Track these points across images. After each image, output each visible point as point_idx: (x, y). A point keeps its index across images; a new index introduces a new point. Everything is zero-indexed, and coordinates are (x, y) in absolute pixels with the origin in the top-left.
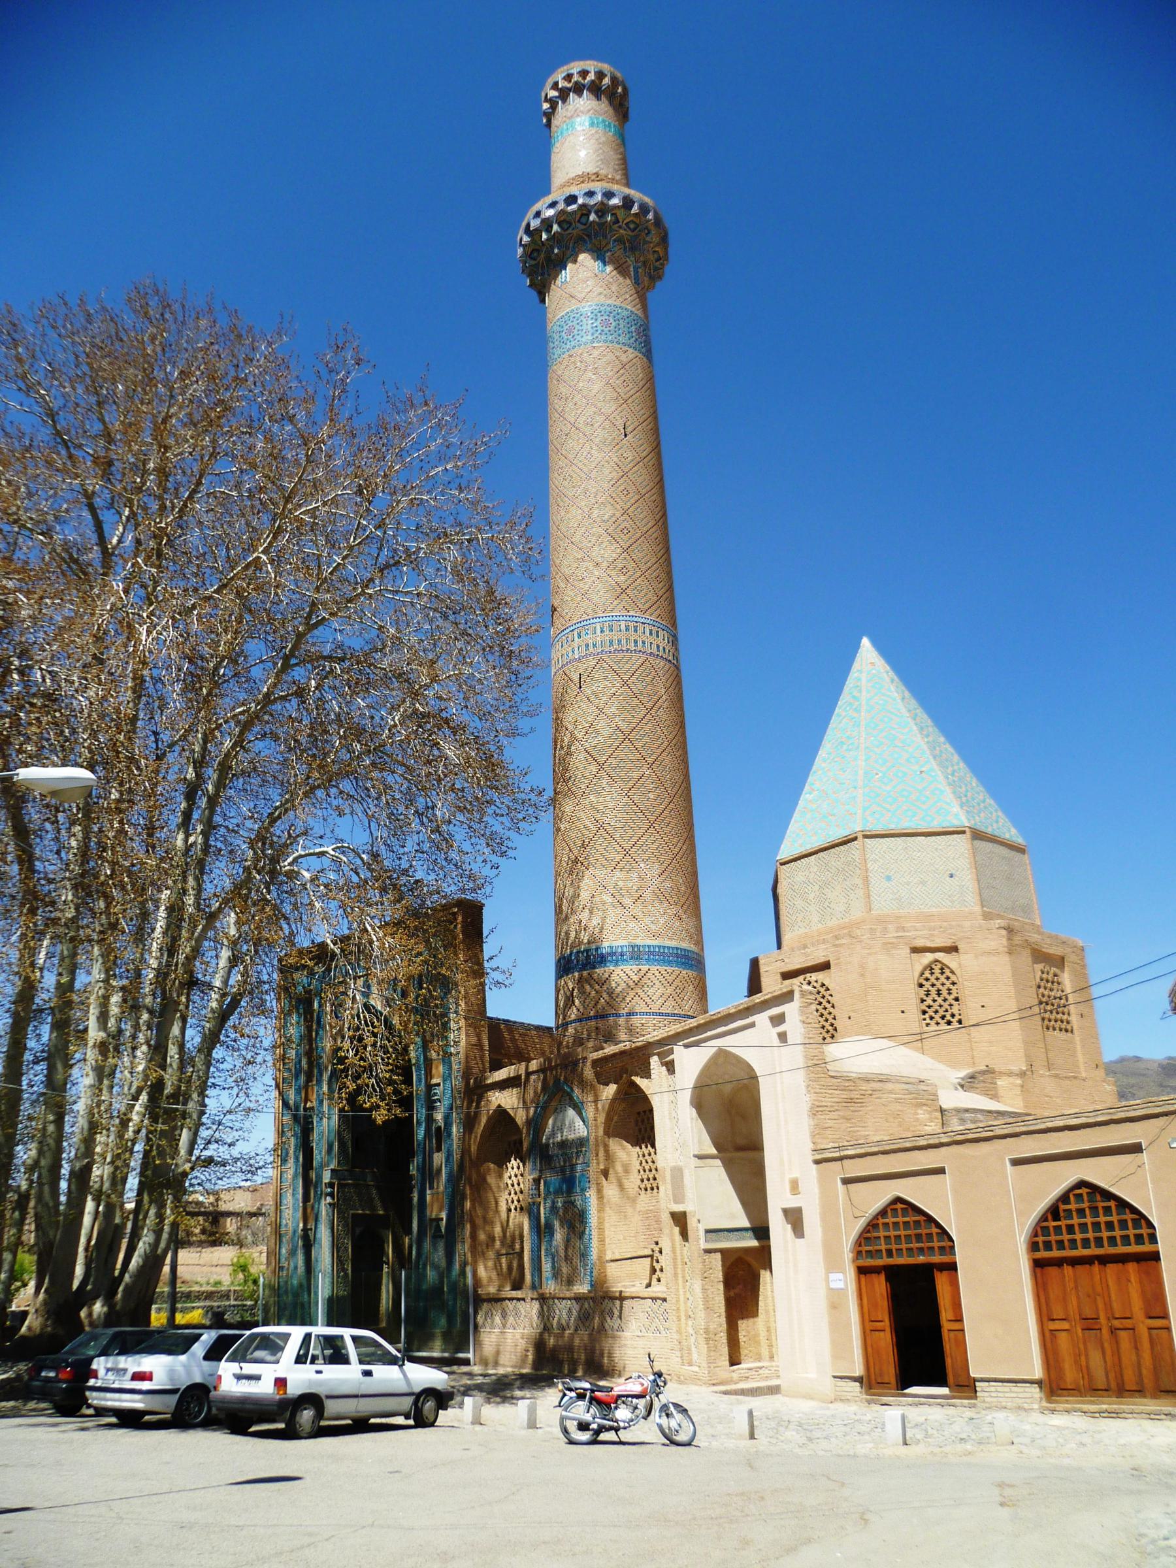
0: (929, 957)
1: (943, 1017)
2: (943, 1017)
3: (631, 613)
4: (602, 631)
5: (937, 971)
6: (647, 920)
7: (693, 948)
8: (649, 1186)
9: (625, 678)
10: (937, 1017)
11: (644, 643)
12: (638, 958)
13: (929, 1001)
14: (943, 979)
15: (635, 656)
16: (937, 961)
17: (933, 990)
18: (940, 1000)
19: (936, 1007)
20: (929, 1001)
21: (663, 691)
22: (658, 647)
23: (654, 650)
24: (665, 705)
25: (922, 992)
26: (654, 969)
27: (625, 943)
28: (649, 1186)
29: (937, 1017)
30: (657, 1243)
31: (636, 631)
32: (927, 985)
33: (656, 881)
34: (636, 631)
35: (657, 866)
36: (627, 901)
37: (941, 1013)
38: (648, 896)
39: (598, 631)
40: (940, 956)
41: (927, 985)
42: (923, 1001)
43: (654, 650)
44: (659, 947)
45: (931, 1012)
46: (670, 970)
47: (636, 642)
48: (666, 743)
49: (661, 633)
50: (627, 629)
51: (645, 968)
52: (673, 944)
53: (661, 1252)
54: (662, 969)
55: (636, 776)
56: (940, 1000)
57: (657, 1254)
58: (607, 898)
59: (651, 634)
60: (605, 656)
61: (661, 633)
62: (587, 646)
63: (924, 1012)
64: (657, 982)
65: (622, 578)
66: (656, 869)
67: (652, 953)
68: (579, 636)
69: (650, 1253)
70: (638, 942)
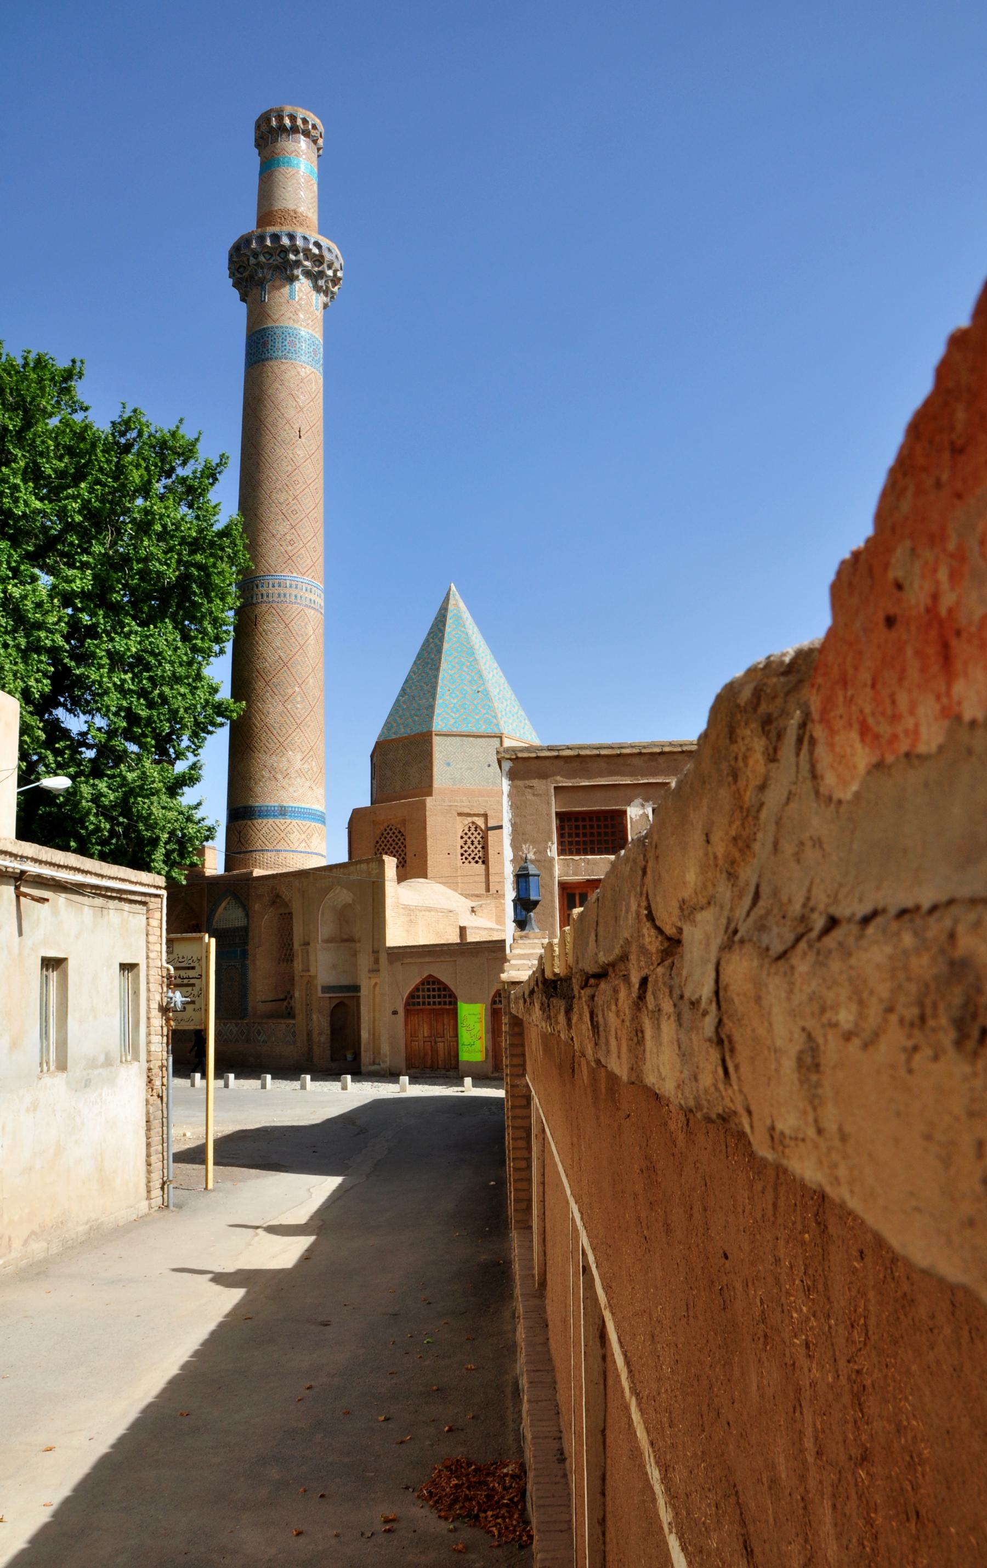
0: (470, 819)
1: (473, 858)
2: (473, 858)
5: (473, 829)
6: (291, 789)
10: (470, 858)
12: (285, 815)
13: (466, 848)
14: (476, 834)
16: (473, 823)
17: (469, 841)
18: (472, 847)
19: (470, 851)
20: (466, 848)
25: (461, 842)
26: (294, 822)
27: (276, 804)
29: (470, 858)
32: (466, 838)
35: (300, 754)
36: (279, 776)
37: (473, 855)
41: (466, 838)
42: (462, 847)
45: (466, 855)
46: (304, 823)
49: (314, 589)
50: (291, 586)
51: (288, 821)
54: (299, 822)
56: (472, 847)
60: (274, 605)
63: (462, 855)
65: (290, 548)
66: (299, 756)
70: (285, 804)
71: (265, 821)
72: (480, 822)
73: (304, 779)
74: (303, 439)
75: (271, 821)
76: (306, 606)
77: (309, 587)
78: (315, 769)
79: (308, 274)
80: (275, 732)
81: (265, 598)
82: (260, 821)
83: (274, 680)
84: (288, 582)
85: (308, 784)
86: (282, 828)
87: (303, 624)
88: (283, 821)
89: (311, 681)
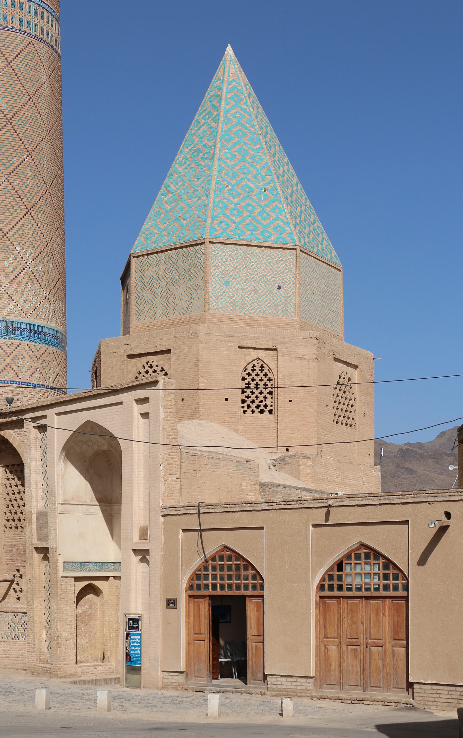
6: (20, 299)
7: (60, 329)
8: (14, 526)
9: (10, 59)
11: (29, 23)
12: (11, 333)
15: (20, 37)
21: (45, 77)
22: (42, 30)
23: (38, 33)
24: (47, 92)
26: (25, 343)
28: (14, 526)
30: (18, 571)
38: (22, 278)
43: (38, 33)
46: (38, 345)
47: (21, 21)
48: (45, 133)
49: (46, 14)
52: (43, 323)
53: (21, 577)
54: (32, 344)
55: (16, 161)
57: (17, 579)
59: (36, 14)
61: (46, 14)
64: (27, 356)
66: (30, 254)
67: (23, 330)
69: (12, 578)
70: (12, 319)
73: (37, 286)
76: (35, 37)
77: (40, 10)
88: (8, 342)
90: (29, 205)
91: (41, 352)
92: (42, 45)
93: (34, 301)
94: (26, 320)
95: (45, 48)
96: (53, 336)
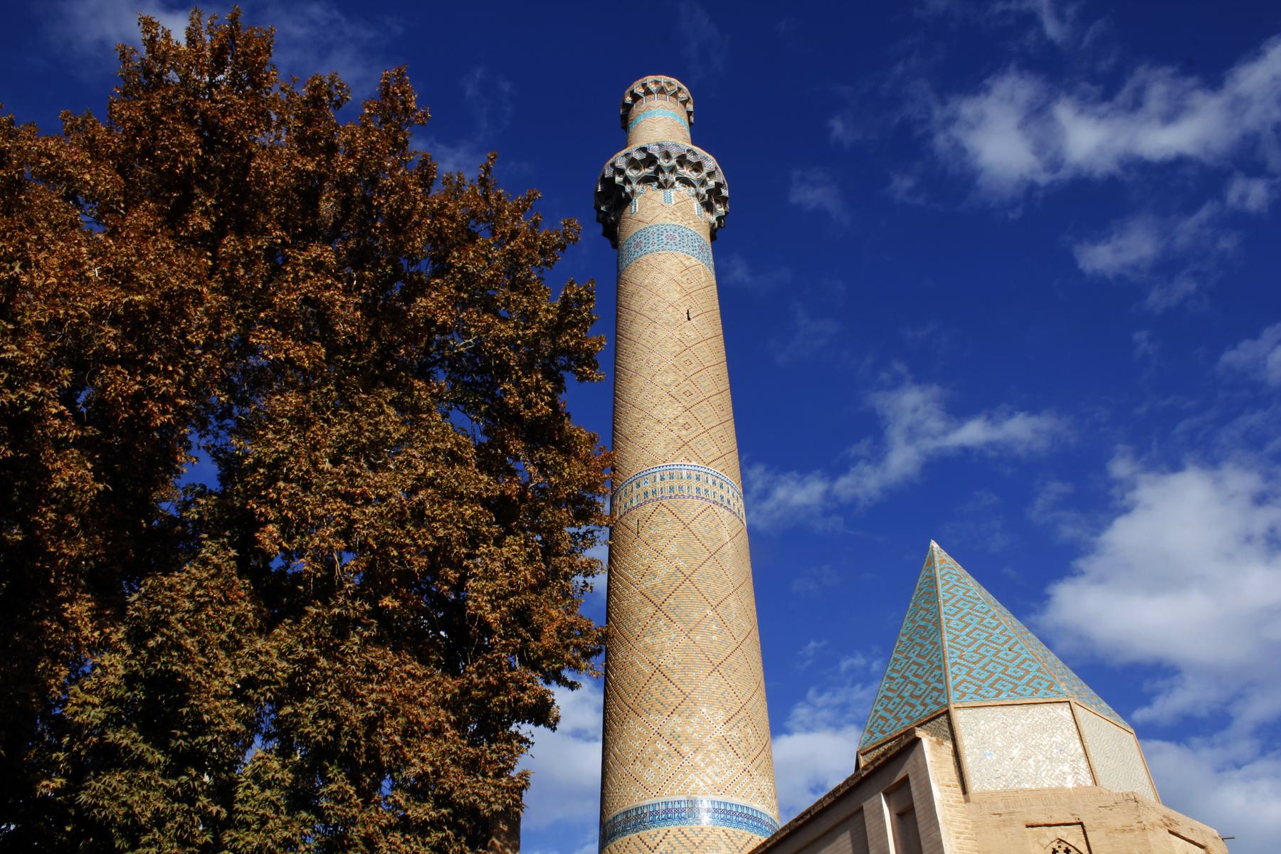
3: (694, 463)
4: (662, 479)
9: (687, 522)
11: (706, 491)
15: (697, 502)
27: (683, 798)
31: (698, 479)
33: (720, 731)
34: (698, 479)
35: (721, 712)
36: (685, 749)
39: (658, 479)
40: (1061, 832)
43: (718, 499)
44: (725, 804)
46: (740, 832)
47: (698, 489)
49: (725, 485)
50: (689, 477)
52: (744, 802)
54: (730, 830)
55: (696, 616)
58: (661, 746)
59: (714, 483)
62: (646, 494)
64: (723, 847)
65: (684, 432)
66: (721, 716)
68: (638, 486)
71: (663, 830)
72: (1073, 837)
73: (732, 754)
74: (693, 321)
75: (673, 829)
78: (753, 741)
79: (686, 182)
80: (675, 678)
81: (650, 496)
82: (653, 831)
83: (671, 600)
84: (684, 473)
85: (740, 763)
86: (697, 841)
87: (712, 525)
89: (733, 605)
90: (716, 662)
91: (744, 841)
92: (722, 510)
93: (729, 774)
94: (720, 798)
95: (727, 513)
96: (760, 820)
